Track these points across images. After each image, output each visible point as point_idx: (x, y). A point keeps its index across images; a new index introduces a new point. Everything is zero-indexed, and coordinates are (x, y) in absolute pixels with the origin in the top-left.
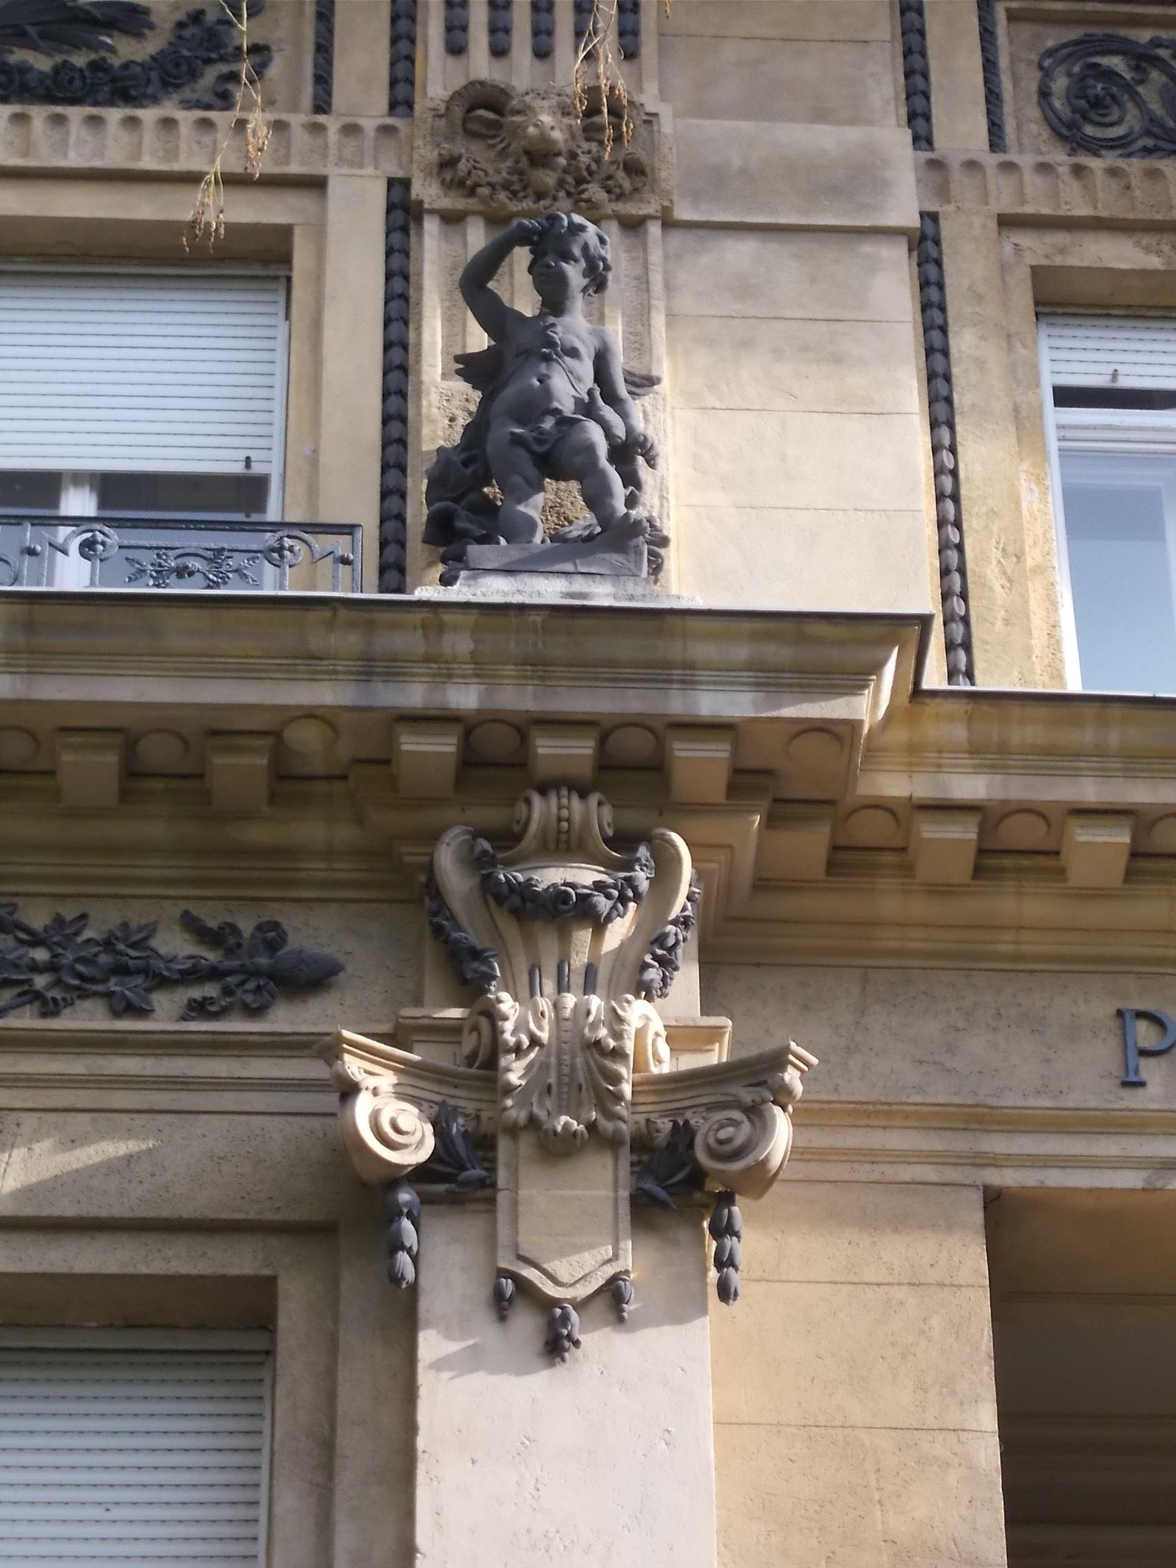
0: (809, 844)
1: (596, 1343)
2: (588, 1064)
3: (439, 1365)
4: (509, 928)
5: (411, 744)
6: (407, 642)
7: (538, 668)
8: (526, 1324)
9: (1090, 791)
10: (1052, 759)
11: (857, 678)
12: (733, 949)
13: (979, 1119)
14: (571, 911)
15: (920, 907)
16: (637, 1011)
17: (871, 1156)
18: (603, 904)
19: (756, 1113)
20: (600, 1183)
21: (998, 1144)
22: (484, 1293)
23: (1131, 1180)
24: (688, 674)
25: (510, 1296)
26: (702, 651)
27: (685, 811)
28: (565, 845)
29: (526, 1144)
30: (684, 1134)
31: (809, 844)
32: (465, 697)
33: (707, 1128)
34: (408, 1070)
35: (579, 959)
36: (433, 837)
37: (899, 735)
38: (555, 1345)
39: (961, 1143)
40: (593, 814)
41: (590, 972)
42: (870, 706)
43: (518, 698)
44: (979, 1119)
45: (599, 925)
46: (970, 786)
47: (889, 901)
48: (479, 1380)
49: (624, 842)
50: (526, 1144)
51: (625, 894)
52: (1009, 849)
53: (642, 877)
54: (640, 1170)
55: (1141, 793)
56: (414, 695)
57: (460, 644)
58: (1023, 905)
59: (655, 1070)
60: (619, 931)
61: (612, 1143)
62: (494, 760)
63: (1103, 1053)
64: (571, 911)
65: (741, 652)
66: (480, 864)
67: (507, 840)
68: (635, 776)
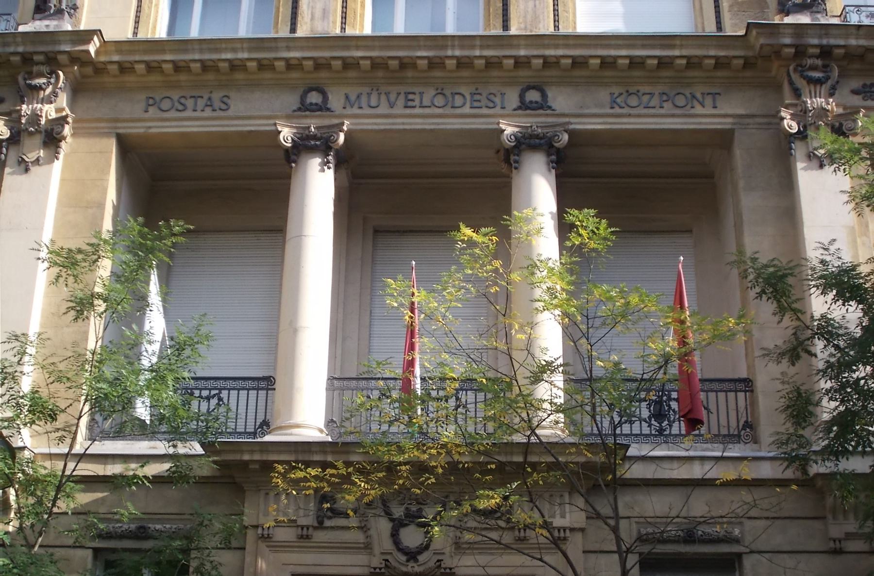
0: (89, 70)
1: (34, 169)
2: (35, 117)
3: (9, 174)
4: (29, 91)
5: (12, 58)
6: (10, 39)
7: (33, 43)
8: (23, 166)
9: (137, 58)
10: (131, 52)
11: (89, 41)
12: (77, 91)
13: (117, 120)
14: (40, 88)
15: (112, 80)
16: (47, 107)
17: (97, 128)
18: (44, 86)
19: (63, 127)
20: (38, 139)
21: (119, 125)
22: (16, 161)
23: (142, 130)
24: (59, 42)
25: (21, 162)
26: (61, 38)
27: (61, 67)
28: (41, 75)
29: (26, 134)
30: (52, 130)
31: (89, 70)
32: (20, 49)
33: (57, 129)
34: (6, 121)
35: (41, 96)
36: (19, 73)
37: (103, 49)
38: (27, 170)
39: (114, 125)
40: (44, 69)
41: (43, 99)
42: (92, 48)
43: (30, 49)
44: (117, 120)
45: (44, 90)
46: (116, 58)
47: (106, 79)
48: (15, 176)
49: (51, 73)
50: (26, 134)
51: (49, 83)
52: (124, 68)
53: (52, 80)
54: (46, 136)
55: (146, 58)
56: (12, 49)
57: (19, 39)
58: (129, 79)
59: (50, 118)
60: (49, 90)
61: (40, 132)
62: (27, 59)
63: (143, 105)
64: (40, 88)
65: (68, 38)
66: (25, 79)
67: (31, 75)
68: (52, 63)
